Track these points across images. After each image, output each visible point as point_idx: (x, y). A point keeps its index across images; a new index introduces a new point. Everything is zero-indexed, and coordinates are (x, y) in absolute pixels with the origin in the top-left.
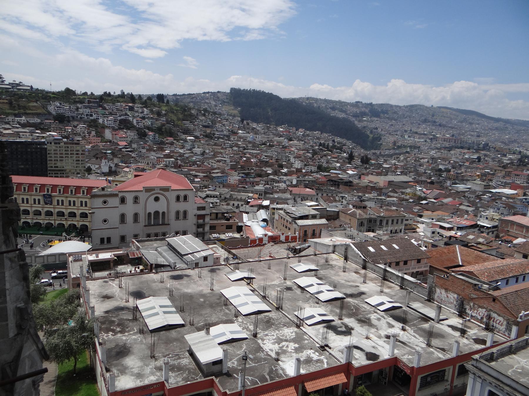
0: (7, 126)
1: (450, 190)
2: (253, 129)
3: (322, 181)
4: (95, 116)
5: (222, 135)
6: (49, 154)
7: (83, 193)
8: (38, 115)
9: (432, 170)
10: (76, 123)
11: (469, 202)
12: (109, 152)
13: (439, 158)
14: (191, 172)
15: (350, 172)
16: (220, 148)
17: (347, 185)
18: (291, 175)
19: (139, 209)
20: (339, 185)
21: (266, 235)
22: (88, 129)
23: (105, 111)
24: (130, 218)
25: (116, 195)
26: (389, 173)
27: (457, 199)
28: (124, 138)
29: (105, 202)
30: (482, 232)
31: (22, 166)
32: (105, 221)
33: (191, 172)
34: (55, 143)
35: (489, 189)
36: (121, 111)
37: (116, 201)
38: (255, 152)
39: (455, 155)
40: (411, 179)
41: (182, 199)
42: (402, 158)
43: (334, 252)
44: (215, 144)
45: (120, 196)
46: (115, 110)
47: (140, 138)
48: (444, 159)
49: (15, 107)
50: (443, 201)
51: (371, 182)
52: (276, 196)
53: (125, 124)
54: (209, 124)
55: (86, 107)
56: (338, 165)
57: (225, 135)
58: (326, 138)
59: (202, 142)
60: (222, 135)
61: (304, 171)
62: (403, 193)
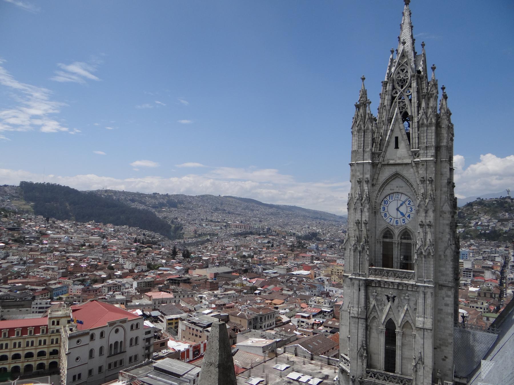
1: (266, 276)
2: (61, 228)
3: (160, 281)
5: (31, 237)
7: (18, 334)
9: (237, 256)
11: (287, 287)
13: (241, 246)
14: (26, 286)
15: (178, 268)
16: (39, 253)
17: (186, 283)
18: (125, 277)
19: (104, 343)
20: (179, 284)
21: (191, 346)
24: (96, 353)
25: (87, 333)
26: (210, 265)
27: (278, 285)
29: (78, 342)
30: (326, 316)
32: (77, 359)
33: (26, 286)
35: (290, 271)
37: (86, 339)
38: (79, 255)
39: (254, 242)
40: (230, 270)
41: (134, 328)
42: (210, 248)
43: (284, 352)
44: (31, 250)
45: (90, 334)
48: (246, 246)
50: (268, 288)
51: (200, 276)
52: (137, 304)
54: (14, 226)
56: (164, 261)
57: (33, 238)
58: (135, 232)
59: (14, 248)
60: (31, 237)
61: (136, 271)
62: (233, 284)
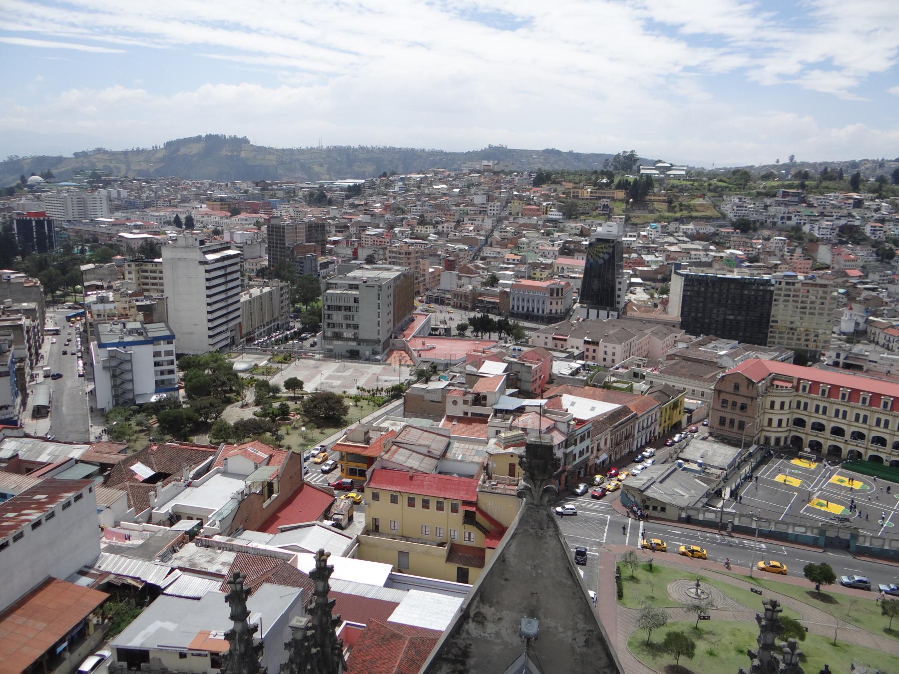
0: (671, 239)
4: (793, 222)
6: (775, 300)
8: (707, 219)
10: (766, 233)
12: (842, 291)
22: (789, 245)
23: (811, 210)
28: (853, 261)
31: (732, 317)
34: (788, 283)
36: (840, 208)
46: (829, 208)
47: (882, 261)
49: (675, 207)
53: (849, 234)
55: (779, 204)
